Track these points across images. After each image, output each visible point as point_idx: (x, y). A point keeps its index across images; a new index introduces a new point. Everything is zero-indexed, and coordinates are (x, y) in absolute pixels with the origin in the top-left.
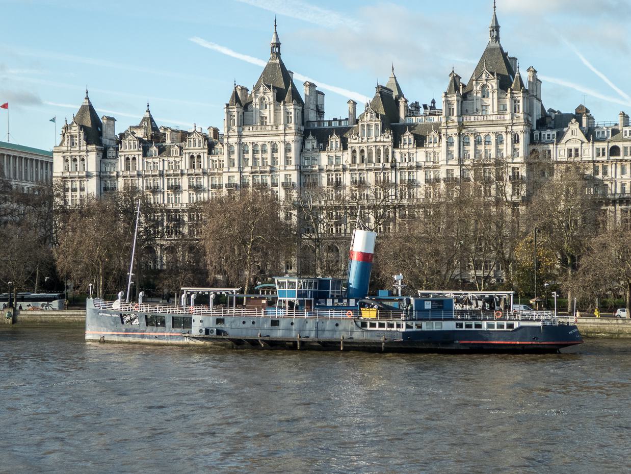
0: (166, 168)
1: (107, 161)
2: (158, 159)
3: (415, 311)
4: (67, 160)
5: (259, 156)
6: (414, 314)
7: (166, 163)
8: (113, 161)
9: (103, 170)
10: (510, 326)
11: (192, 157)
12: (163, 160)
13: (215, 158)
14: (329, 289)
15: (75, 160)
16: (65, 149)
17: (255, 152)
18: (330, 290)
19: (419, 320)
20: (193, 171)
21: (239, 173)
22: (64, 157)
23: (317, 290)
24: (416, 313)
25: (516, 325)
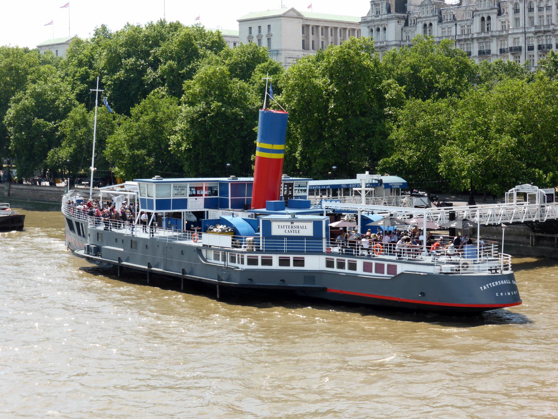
0: (459, 33)
1: (407, 29)
2: (450, 25)
3: (263, 239)
4: (372, 31)
5: (545, 13)
6: (261, 245)
7: (459, 28)
8: (413, 29)
9: (404, 38)
10: (392, 269)
11: (483, 19)
12: (456, 25)
13: (502, 18)
14: (228, 197)
15: (378, 30)
16: (369, 19)
17: (540, 9)
18: (230, 198)
19: (267, 252)
20: (483, 35)
21: (524, 35)
22: (369, 27)
23: (218, 197)
24: (263, 242)
25: (401, 268)
